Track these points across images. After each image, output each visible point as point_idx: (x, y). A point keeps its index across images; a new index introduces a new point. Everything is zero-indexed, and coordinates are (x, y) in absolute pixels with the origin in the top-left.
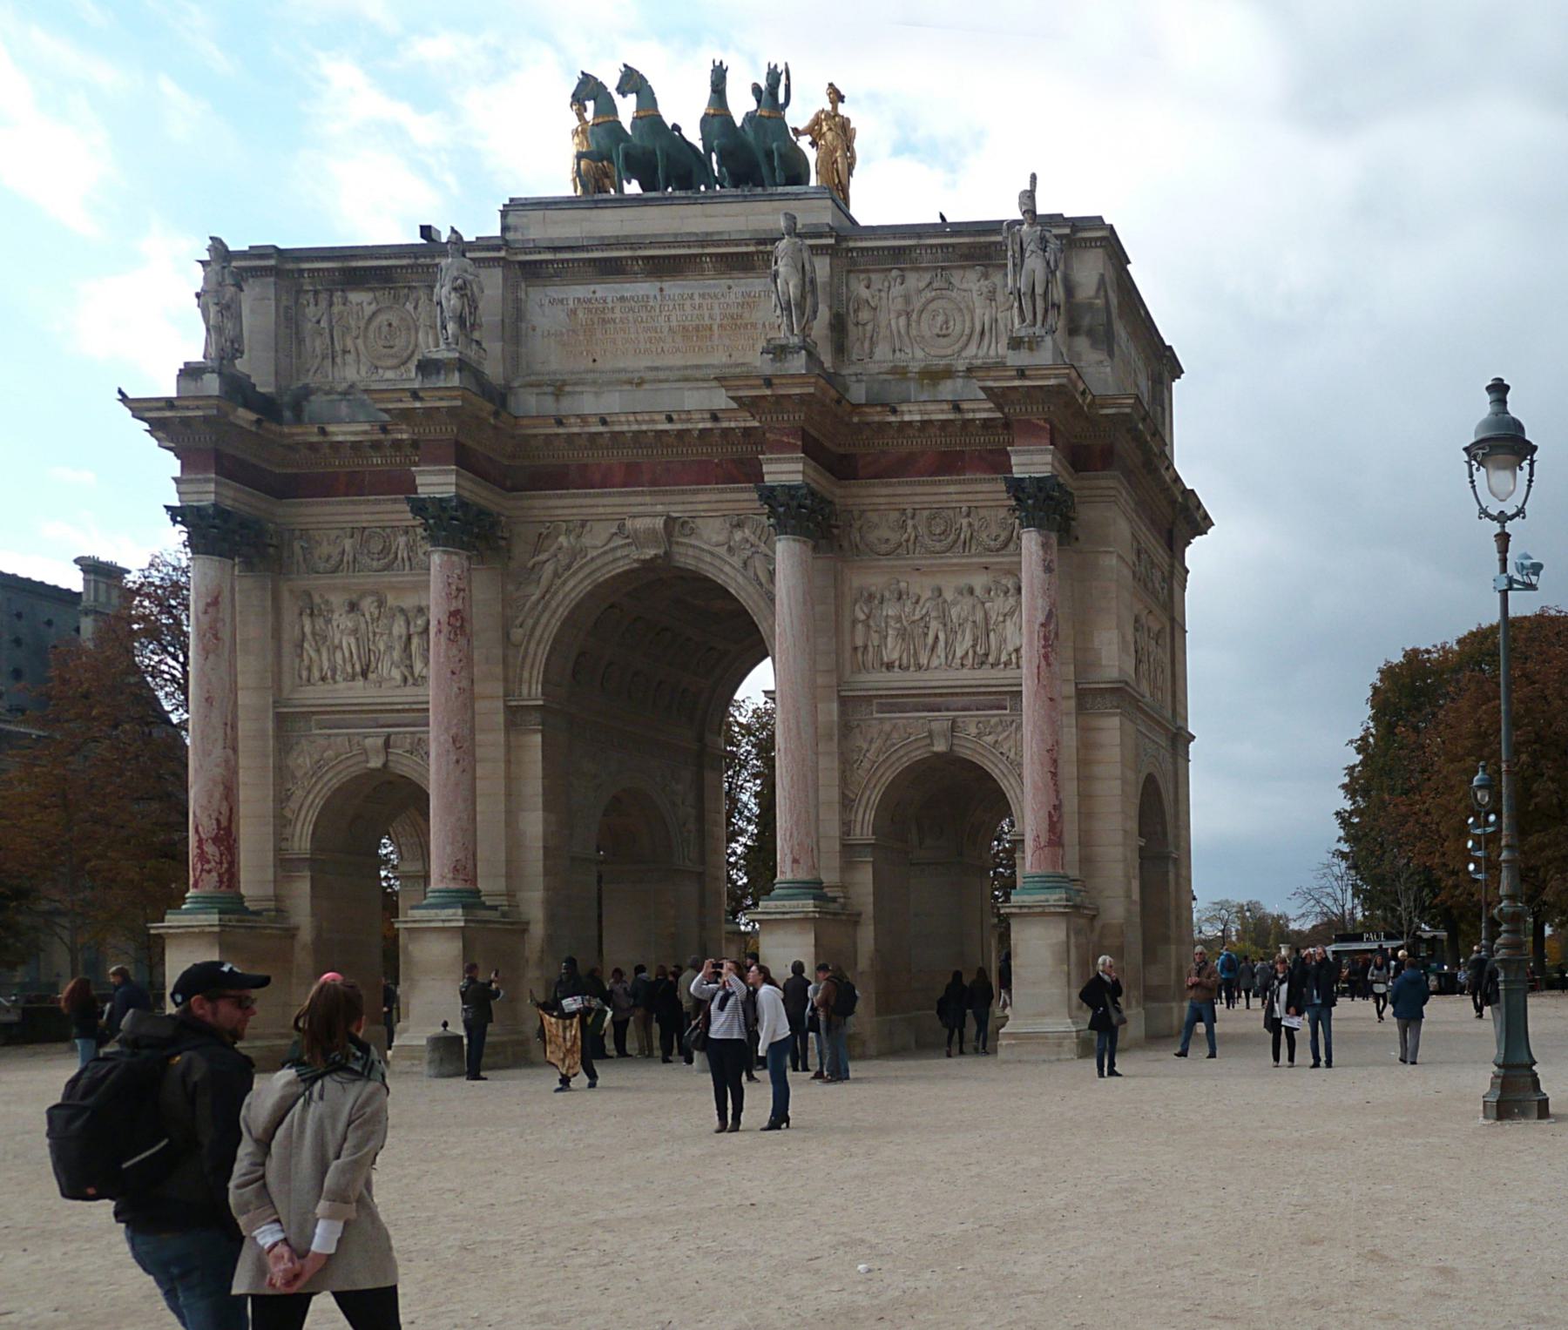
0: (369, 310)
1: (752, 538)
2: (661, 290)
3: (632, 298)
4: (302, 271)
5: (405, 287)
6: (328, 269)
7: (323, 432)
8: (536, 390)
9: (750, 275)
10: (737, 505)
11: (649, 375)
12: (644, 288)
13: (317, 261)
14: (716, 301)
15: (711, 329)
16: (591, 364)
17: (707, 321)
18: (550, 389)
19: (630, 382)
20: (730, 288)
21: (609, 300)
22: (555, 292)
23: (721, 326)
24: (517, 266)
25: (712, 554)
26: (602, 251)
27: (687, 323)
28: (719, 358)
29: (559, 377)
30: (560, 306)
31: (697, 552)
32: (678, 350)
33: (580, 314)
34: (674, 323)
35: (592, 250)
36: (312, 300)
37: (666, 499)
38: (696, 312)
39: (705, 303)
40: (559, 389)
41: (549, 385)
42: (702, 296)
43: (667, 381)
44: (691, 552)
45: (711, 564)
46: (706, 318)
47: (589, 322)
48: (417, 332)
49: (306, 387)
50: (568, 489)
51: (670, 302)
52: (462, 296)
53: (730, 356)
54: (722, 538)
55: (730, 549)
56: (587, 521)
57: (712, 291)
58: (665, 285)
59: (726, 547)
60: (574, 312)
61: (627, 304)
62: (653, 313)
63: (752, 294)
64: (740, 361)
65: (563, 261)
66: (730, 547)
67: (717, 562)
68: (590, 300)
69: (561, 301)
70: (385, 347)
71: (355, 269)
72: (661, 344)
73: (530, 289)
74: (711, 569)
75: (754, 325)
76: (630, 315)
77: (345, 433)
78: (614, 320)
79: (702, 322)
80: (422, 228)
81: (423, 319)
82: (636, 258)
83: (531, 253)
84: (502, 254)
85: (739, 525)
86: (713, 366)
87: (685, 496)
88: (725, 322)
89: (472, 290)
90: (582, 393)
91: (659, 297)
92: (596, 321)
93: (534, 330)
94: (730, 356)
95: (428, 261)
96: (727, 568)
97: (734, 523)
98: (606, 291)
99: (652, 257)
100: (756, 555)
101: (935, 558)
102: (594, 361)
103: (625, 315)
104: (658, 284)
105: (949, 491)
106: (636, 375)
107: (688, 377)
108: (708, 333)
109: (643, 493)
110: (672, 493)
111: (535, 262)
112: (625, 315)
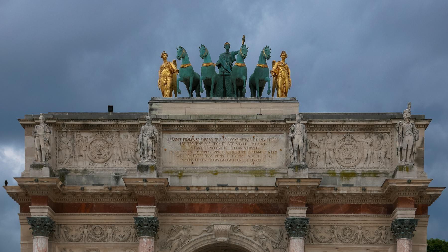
0: (90, 140)
1: (266, 234)
2: (223, 137)
3: (210, 139)
4: (63, 125)
5: (107, 132)
6: (76, 125)
7: (83, 189)
8: (170, 174)
9: (263, 132)
10: (259, 221)
11: (219, 170)
12: (217, 136)
13: (73, 121)
14: (248, 142)
15: (245, 152)
16: (190, 165)
17: (243, 149)
18: (177, 174)
19: (212, 173)
20: (254, 137)
21: (200, 140)
22: (175, 136)
23: (249, 152)
24: (161, 126)
25: (248, 240)
26: (202, 122)
27: (234, 150)
28: (248, 164)
29: (179, 169)
30: (177, 142)
31: (241, 239)
32: (230, 160)
33: (187, 145)
34: (229, 150)
35: (197, 121)
36: (65, 135)
37: (229, 218)
38: (238, 146)
39: (242, 142)
40: (180, 175)
41: (176, 173)
42: (241, 140)
43: (228, 173)
44: (238, 239)
45: (247, 243)
46: (243, 148)
47: (190, 148)
48: (113, 148)
49: (64, 169)
50: (184, 213)
51: (227, 141)
52: (153, 140)
53: (253, 163)
54: (252, 233)
55: (256, 238)
56: (192, 225)
57: (246, 138)
58: (225, 135)
59: (254, 237)
60: (183, 144)
61: (207, 141)
62: (219, 146)
63: (264, 140)
64: (258, 165)
65: (182, 125)
66: (255, 237)
67: (250, 243)
68: (191, 140)
69: (178, 139)
70: (98, 155)
71: (88, 125)
72: (223, 158)
73: (164, 134)
74: (247, 245)
75: (264, 152)
76: (209, 146)
77: (92, 190)
78: (202, 148)
79: (241, 150)
80: (109, 107)
81: (117, 144)
82: (215, 125)
83: (169, 121)
84: (159, 122)
85: (260, 229)
86: (246, 167)
87: (237, 217)
88: (252, 150)
89: (157, 138)
90: (191, 176)
91: (222, 140)
92: (193, 147)
93: (165, 150)
94: (253, 163)
95: (123, 123)
96: (254, 245)
97: (259, 228)
98: (199, 136)
99: (223, 125)
100: (268, 241)
101: (345, 245)
102: (192, 163)
103: (207, 146)
104: (222, 135)
105: (354, 220)
106: (214, 170)
107: (238, 172)
108: (244, 154)
109: (218, 216)
110: (231, 216)
111: (170, 125)
112: (207, 146)
